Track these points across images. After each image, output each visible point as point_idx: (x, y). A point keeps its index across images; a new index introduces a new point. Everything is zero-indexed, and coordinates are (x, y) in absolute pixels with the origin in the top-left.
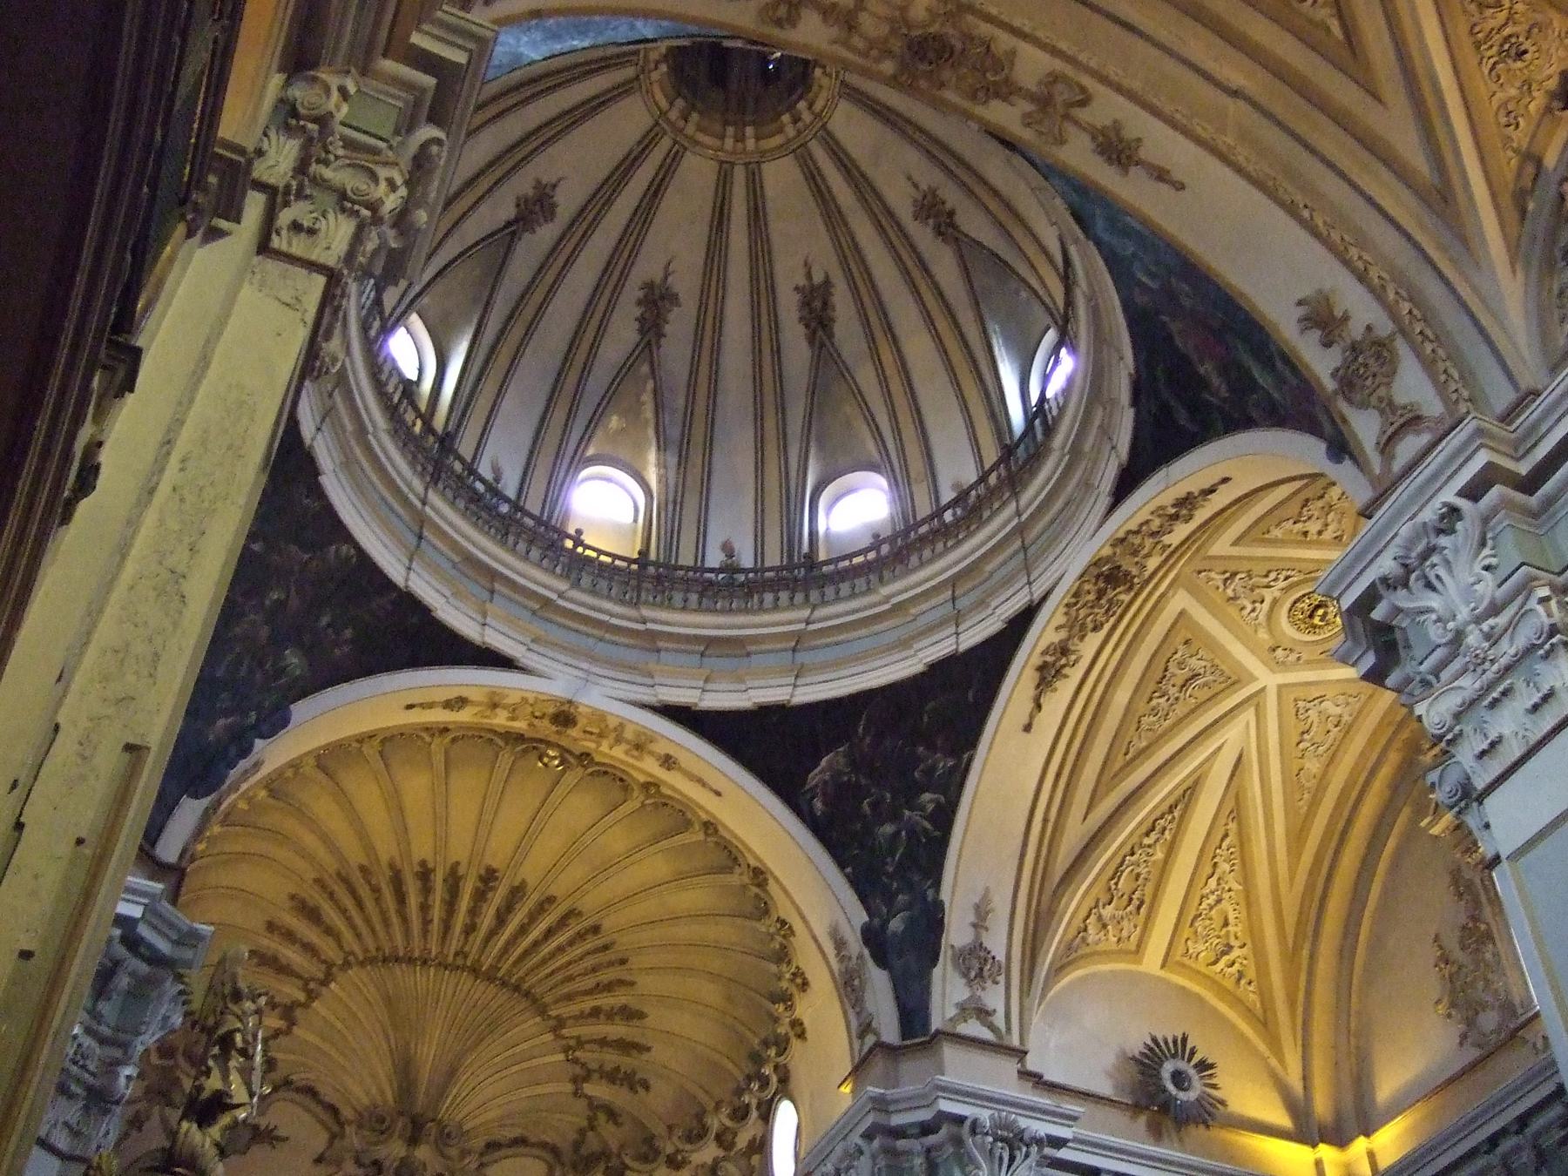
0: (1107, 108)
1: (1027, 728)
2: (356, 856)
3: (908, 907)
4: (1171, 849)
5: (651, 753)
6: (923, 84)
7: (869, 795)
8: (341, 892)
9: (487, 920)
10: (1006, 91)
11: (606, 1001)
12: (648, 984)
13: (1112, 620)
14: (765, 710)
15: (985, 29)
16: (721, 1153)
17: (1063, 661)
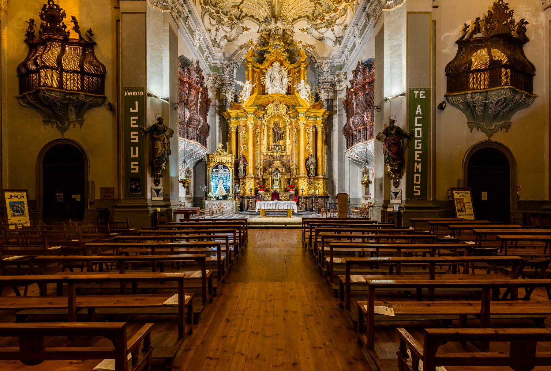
16: (346, 4)
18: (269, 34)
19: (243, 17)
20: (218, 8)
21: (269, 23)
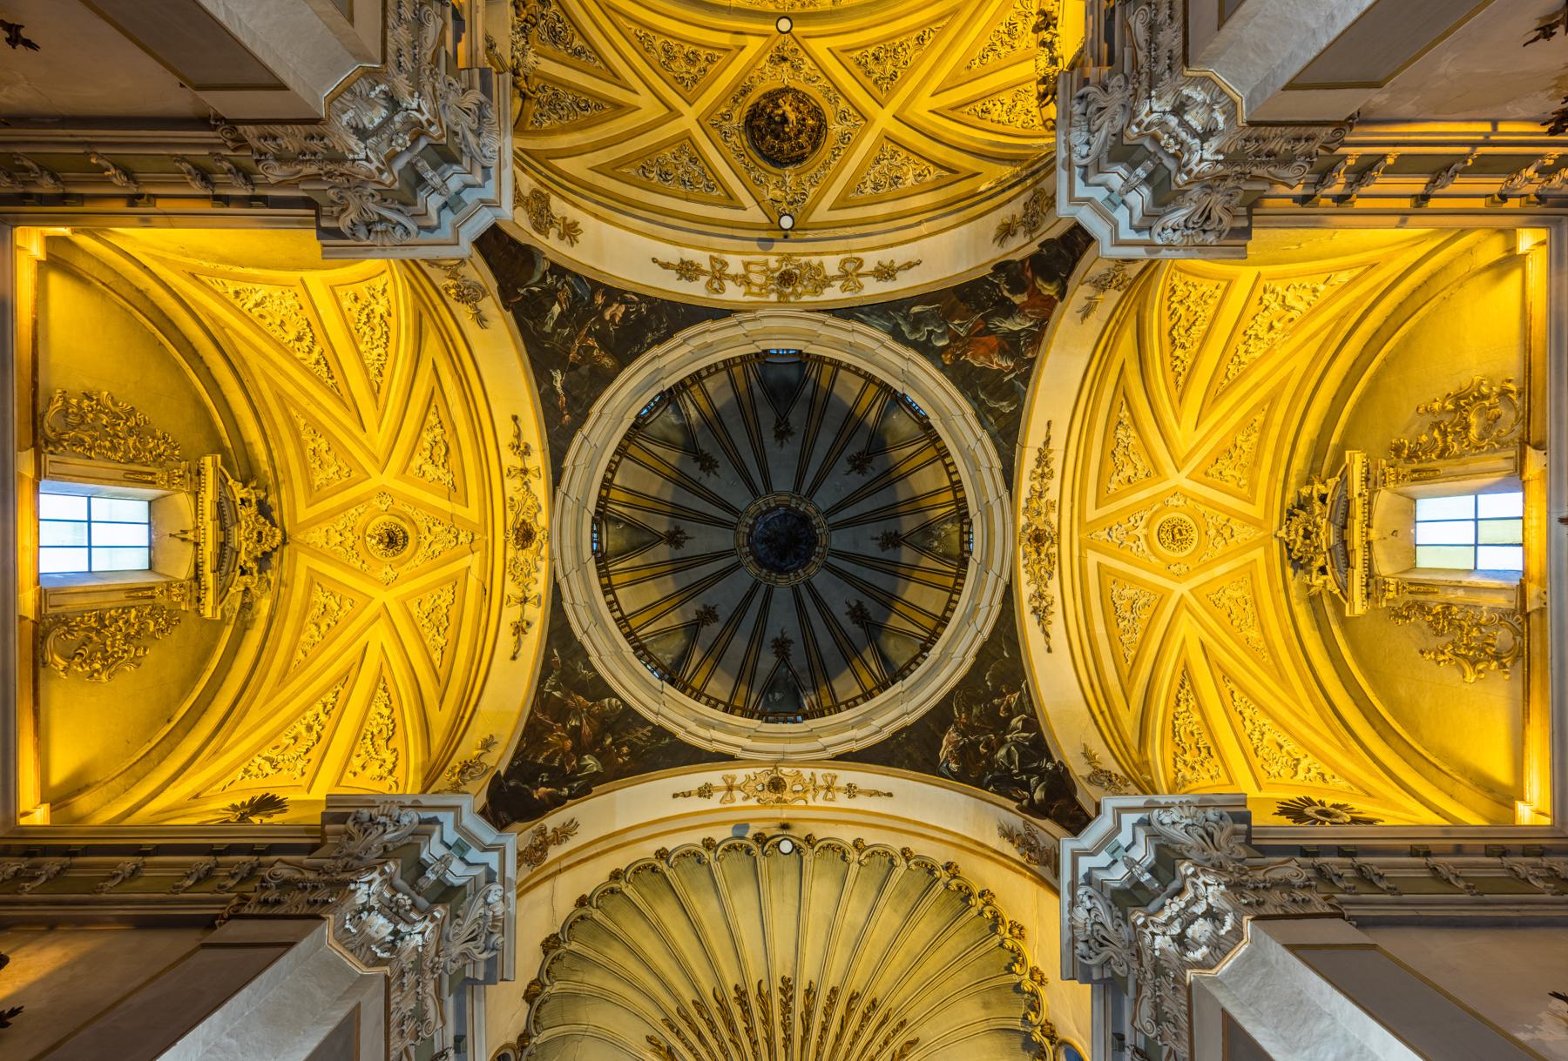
0: (871, 260)
1: (1049, 650)
4: (1201, 709)
5: (839, 789)
6: (792, 299)
7: (981, 742)
8: (683, 1025)
10: (827, 282)
13: (1056, 566)
14: (896, 734)
15: (804, 259)
17: (1044, 604)
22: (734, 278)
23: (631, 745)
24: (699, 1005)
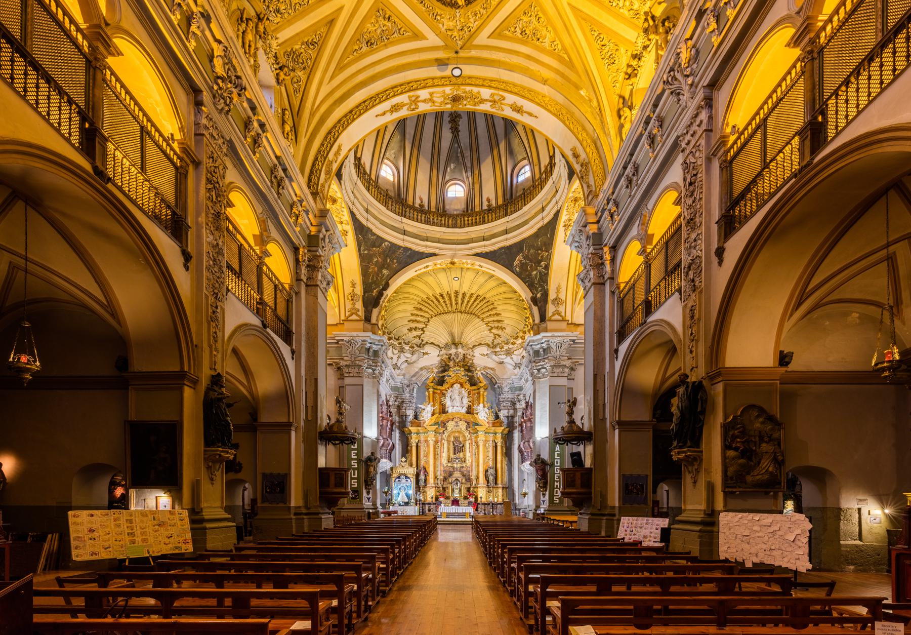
2: (424, 297)
3: (541, 291)
8: (424, 303)
9: (460, 301)
10: (482, 101)
11: (492, 313)
12: (500, 308)
14: (501, 249)
18: (449, 358)
19: (424, 345)
20: (400, 341)
21: (450, 349)
22: (425, 101)
23: (397, 258)
24: (429, 298)
